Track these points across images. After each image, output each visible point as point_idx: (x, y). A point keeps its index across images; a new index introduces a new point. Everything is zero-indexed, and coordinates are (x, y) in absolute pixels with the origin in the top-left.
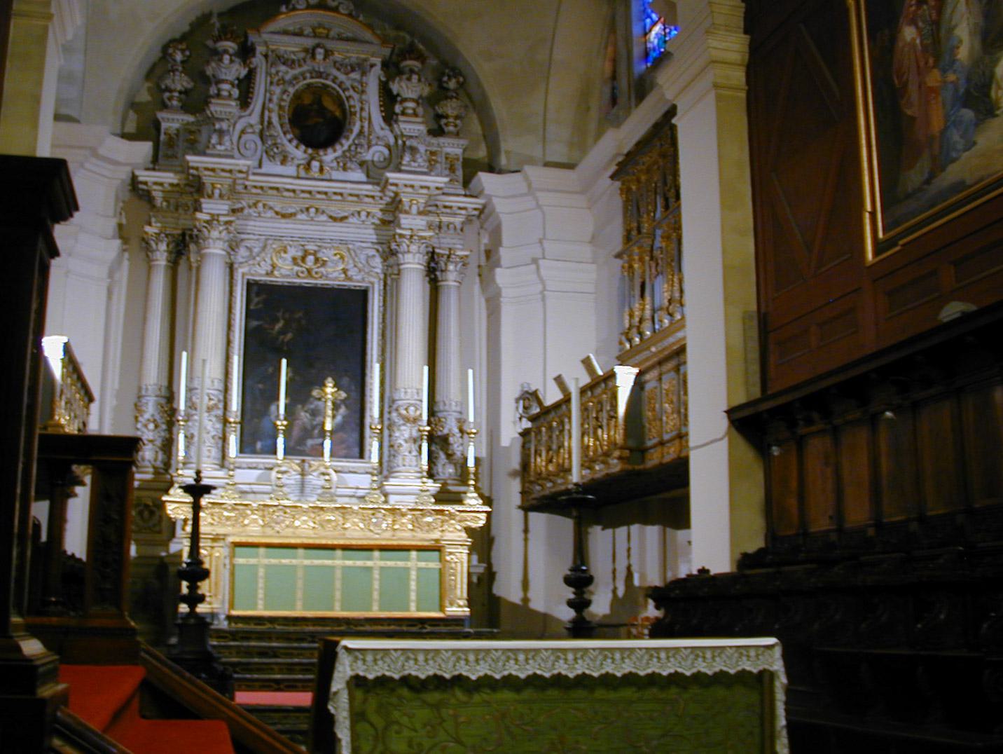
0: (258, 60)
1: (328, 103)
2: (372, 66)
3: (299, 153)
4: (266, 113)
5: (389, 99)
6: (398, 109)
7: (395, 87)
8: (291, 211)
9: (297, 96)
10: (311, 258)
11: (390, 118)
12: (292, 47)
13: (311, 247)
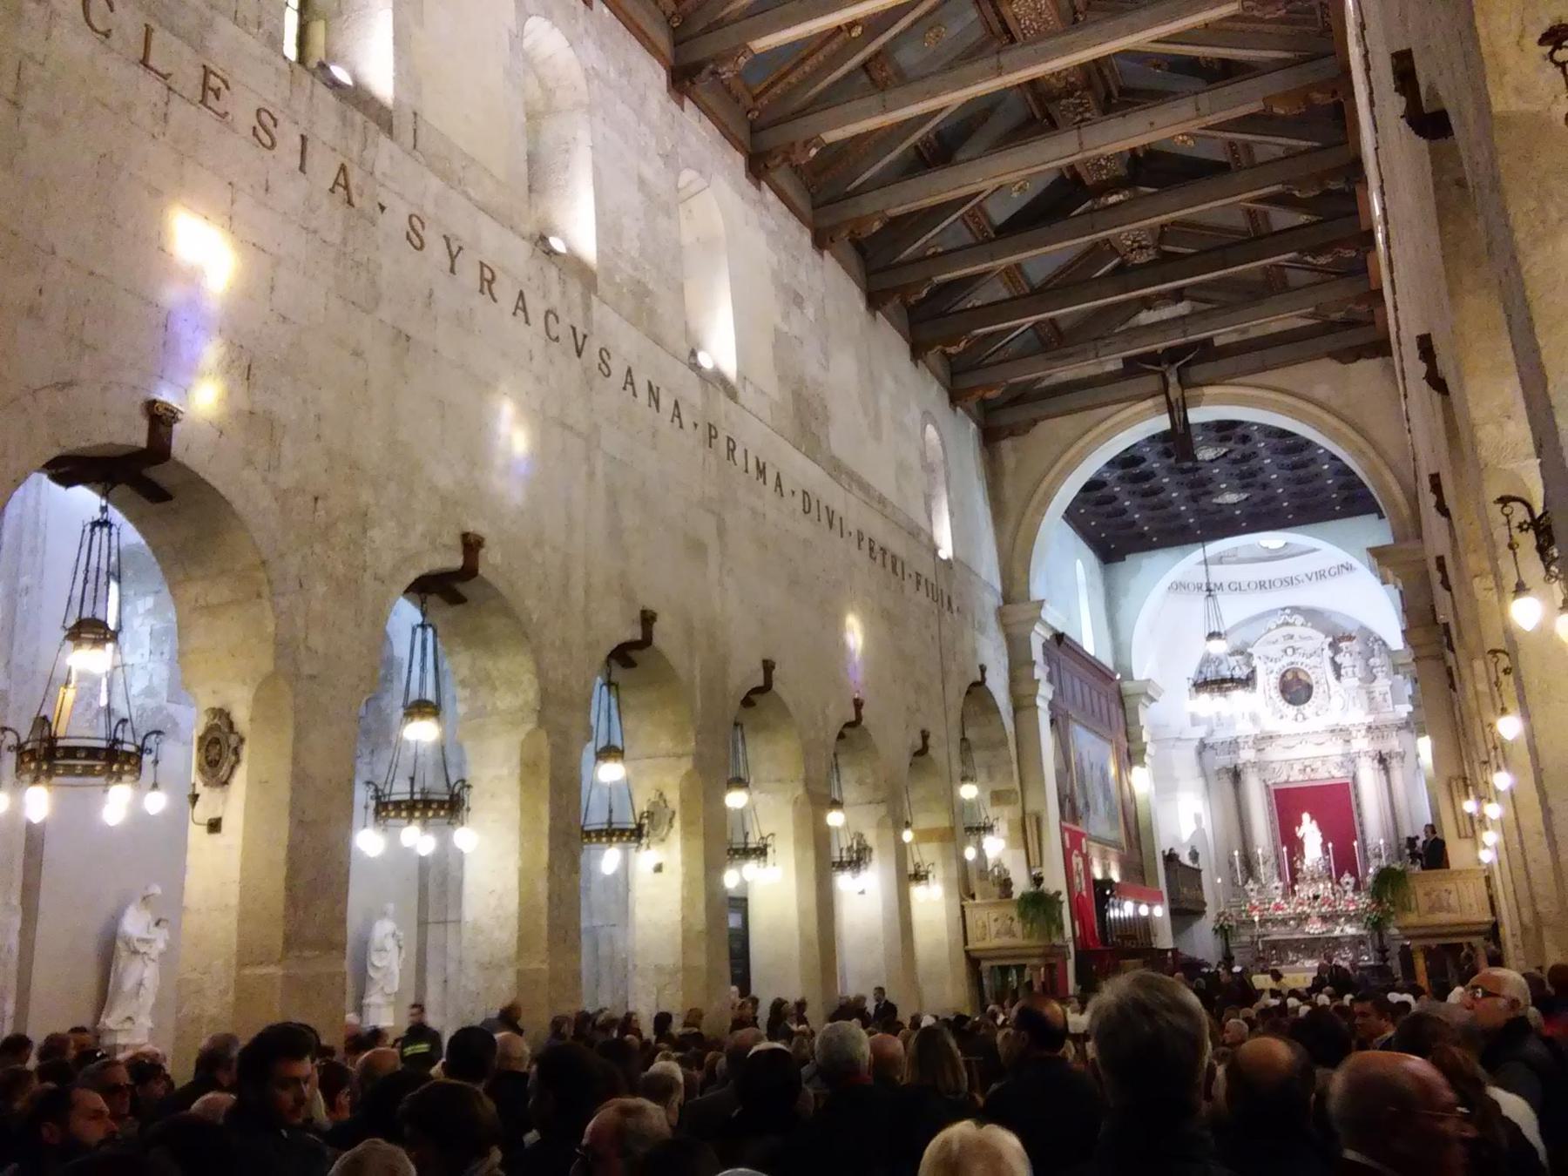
0: (1255, 662)
1: (1301, 676)
2: (1323, 650)
3: (1291, 710)
4: (1267, 693)
5: (1337, 668)
6: (1343, 672)
7: (1338, 659)
8: (1291, 744)
9: (1284, 676)
10: (1308, 770)
11: (1338, 676)
12: (1275, 651)
13: (1307, 763)
